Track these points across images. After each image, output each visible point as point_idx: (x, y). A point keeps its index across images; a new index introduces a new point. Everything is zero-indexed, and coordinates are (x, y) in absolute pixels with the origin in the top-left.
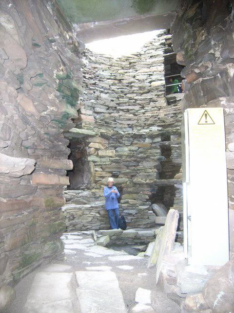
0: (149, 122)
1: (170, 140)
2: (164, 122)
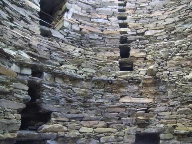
0: (17, 43)
1: (43, 78)
2: (35, 51)
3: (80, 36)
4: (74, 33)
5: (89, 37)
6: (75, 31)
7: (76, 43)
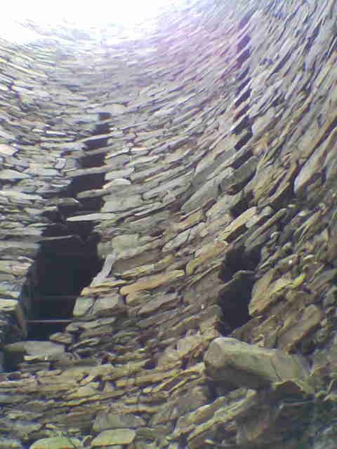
3: (112, 325)
4: (94, 324)
5: (141, 311)
6: (102, 315)
7: (95, 352)
